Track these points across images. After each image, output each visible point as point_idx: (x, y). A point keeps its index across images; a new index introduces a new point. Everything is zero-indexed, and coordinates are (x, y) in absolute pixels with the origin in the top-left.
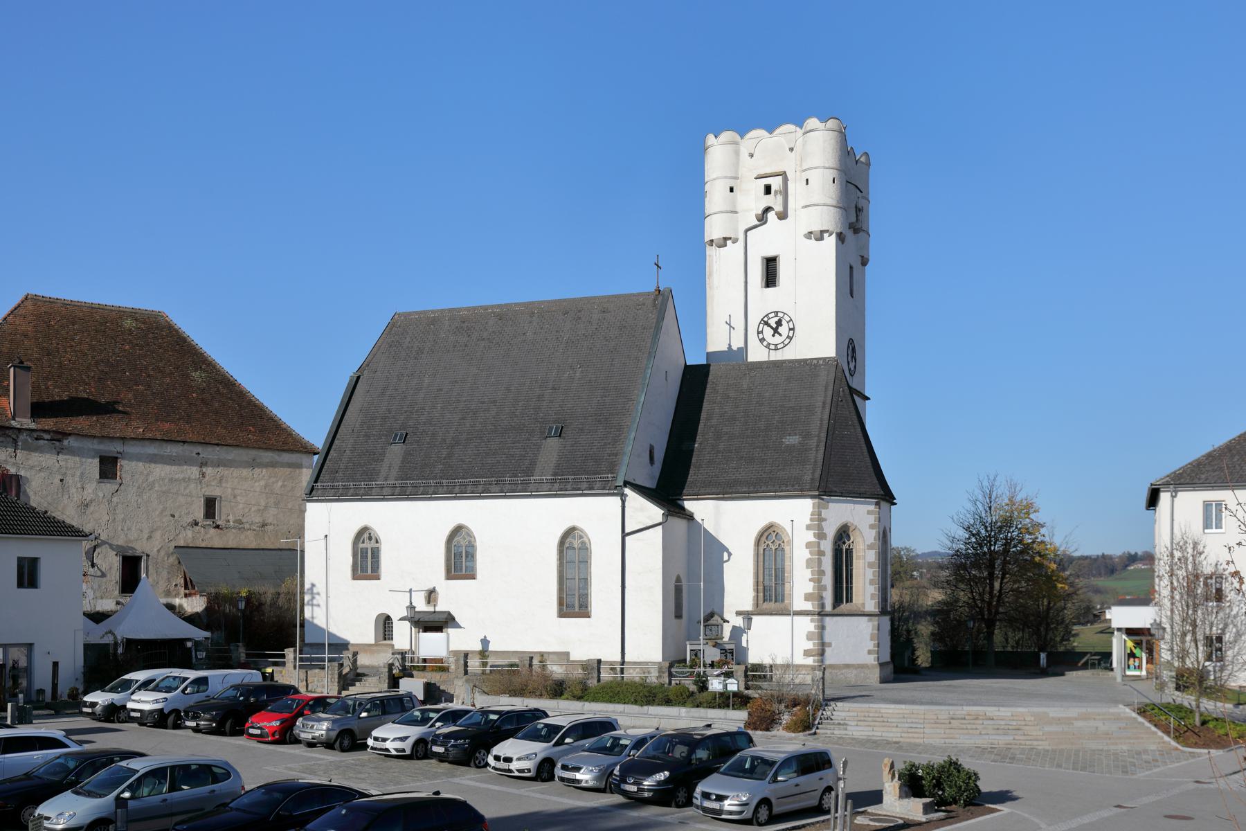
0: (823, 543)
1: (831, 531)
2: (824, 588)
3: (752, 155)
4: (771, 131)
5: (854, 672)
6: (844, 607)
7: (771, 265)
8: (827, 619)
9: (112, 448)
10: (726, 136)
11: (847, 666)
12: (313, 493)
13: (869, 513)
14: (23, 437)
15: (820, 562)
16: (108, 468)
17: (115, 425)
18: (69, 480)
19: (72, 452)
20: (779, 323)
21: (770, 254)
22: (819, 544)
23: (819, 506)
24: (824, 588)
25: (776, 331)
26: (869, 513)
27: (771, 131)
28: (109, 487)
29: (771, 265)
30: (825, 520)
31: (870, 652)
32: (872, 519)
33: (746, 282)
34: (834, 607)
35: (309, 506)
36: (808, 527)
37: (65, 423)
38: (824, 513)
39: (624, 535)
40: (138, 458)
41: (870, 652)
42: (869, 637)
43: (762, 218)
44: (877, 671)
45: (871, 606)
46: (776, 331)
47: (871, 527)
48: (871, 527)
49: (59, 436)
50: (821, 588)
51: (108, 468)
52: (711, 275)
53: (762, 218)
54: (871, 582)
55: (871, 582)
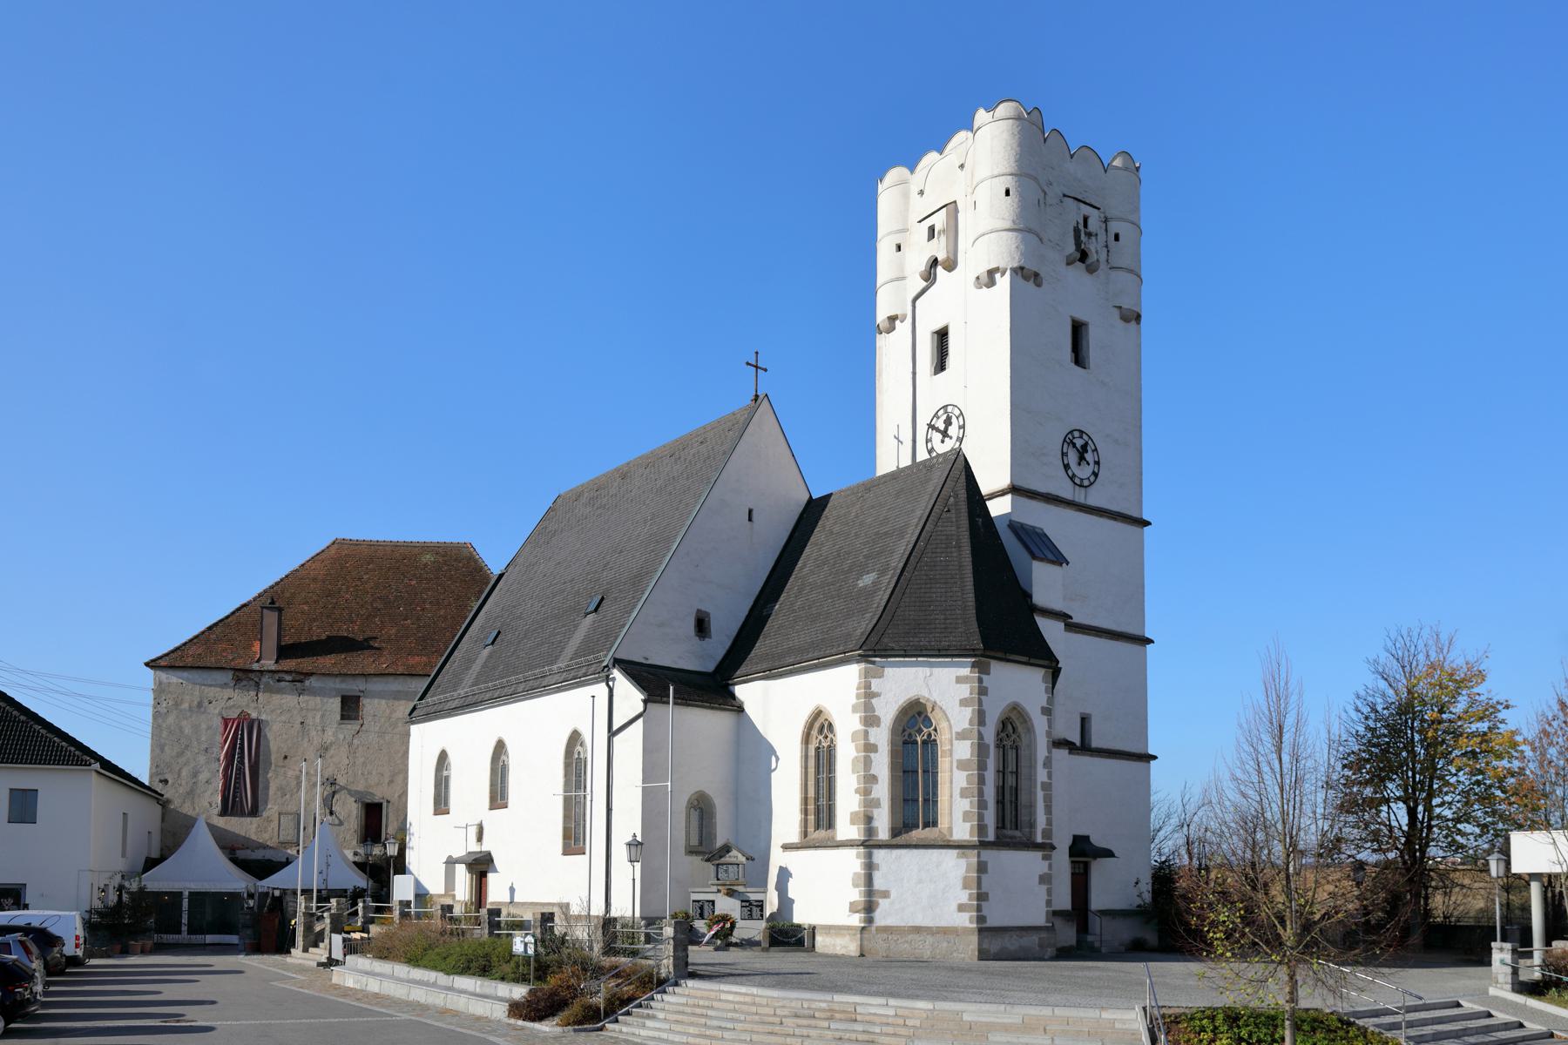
0: (873, 731)
1: (888, 711)
2: (876, 803)
3: (921, 193)
4: (941, 151)
5: (930, 939)
6: (918, 834)
7: (942, 336)
8: (880, 855)
9: (353, 686)
10: (895, 174)
11: (917, 930)
12: (414, 716)
13: (959, 680)
14: (265, 679)
15: (868, 763)
16: (350, 707)
17: (363, 661)
18: (309, 721)
19: (313, 692)
20: (948, 422)
21: (938, 326)
22: (866, 733)
23: (867, 675)
24: (876, 803)
25: (945, 434)
26: (959, 680)
27: (941, 151)
28: (352, 727)
31: (961, 908)
32: (965, 691)
33: (914, 373)
35: (414, 729)
36: (855, 709)
37: (306, 664)
38: (876, 685)
39: (612, 733)
40: (381, 695)
41: (961, 908)
42: (959, 884)
43: (929, 276)
44: (975, 938)
45: (963, 831)
46: (945, 434)
47: (964, 703)
48: (964, 703)
49: (300, 677)
50: (870, 803)
51: (350, 707)
53: (929, 276)
54: (964, 793)
55: (964, 793)
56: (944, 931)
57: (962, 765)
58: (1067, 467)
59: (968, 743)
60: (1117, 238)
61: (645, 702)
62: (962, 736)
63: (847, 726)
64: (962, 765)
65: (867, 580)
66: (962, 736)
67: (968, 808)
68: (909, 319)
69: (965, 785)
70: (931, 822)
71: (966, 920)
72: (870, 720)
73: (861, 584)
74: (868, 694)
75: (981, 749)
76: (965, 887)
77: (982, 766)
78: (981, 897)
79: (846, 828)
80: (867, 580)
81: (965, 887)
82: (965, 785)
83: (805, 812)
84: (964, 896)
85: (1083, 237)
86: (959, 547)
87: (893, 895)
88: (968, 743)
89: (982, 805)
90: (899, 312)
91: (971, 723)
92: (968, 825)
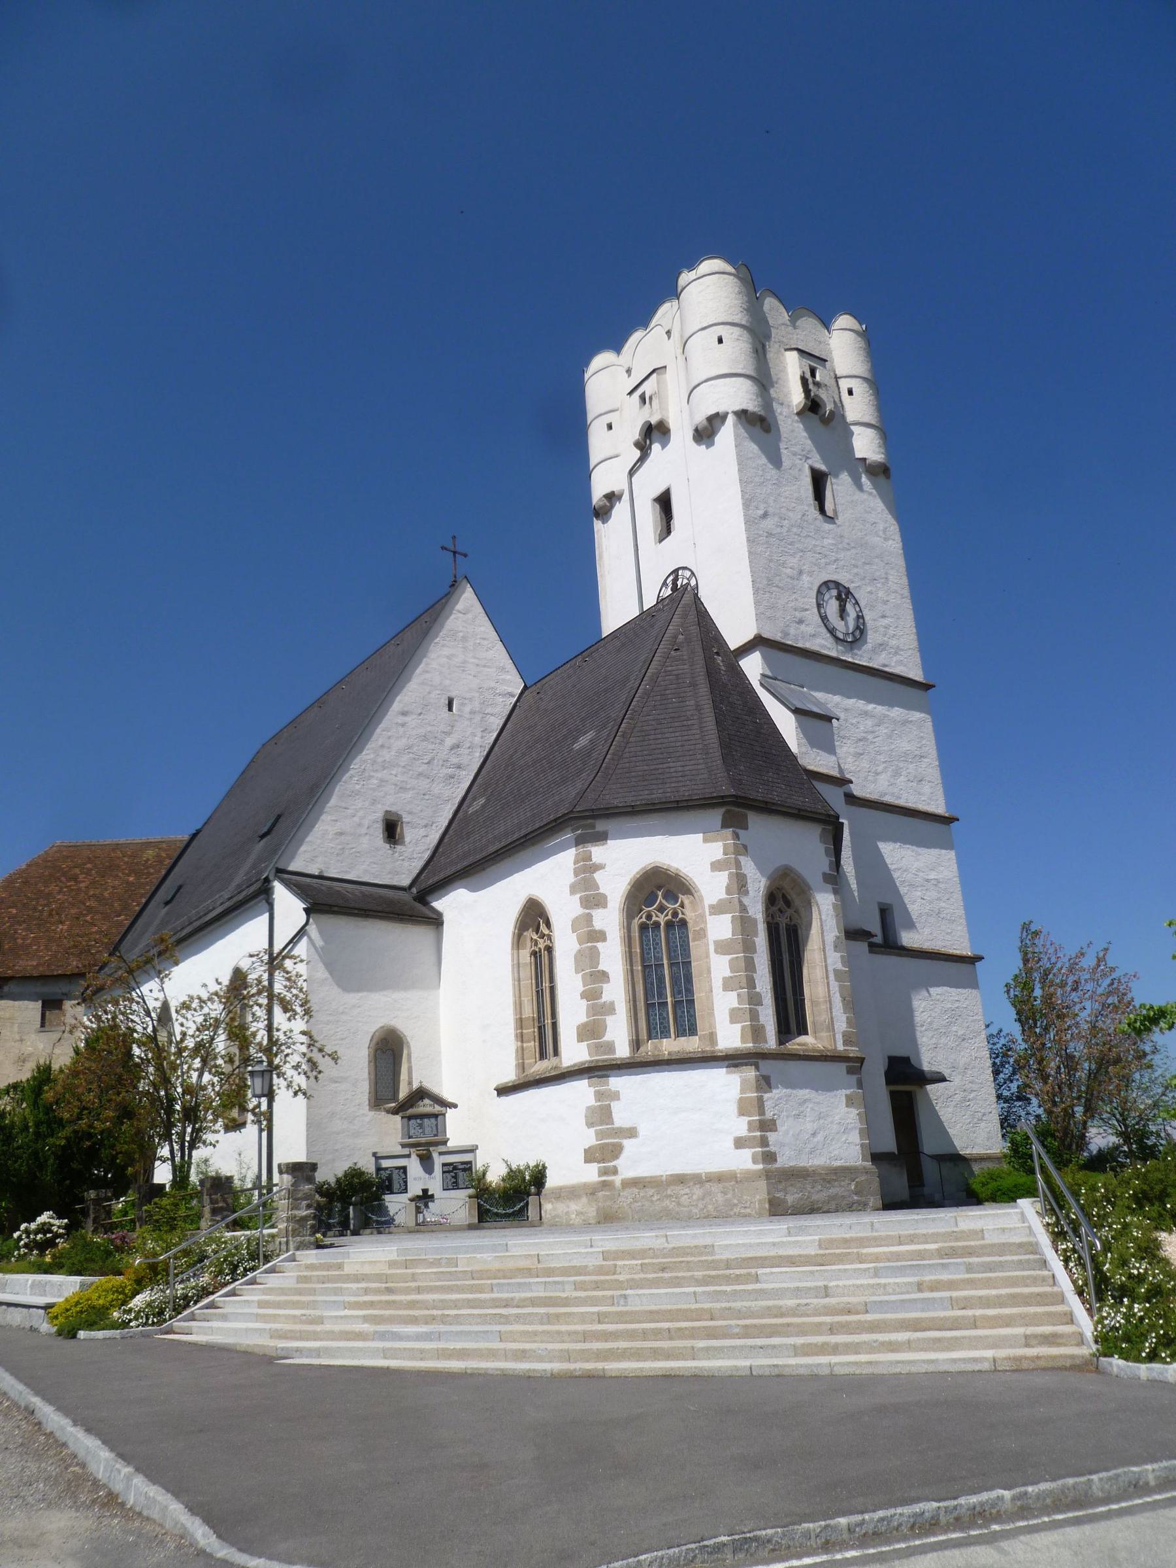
2: (610, 1009)
5: (698, 1192)
7: (664, 502)
8: (616, 1082)
11: (680, 1180)
22: (589, 919)
24: (610, 1009)
29: (664, 502)
30: (599, 867)
31: (739, 1143)
34: (636, 1044)
36: (573, 889)
41: (739, 1143)
42: (733, 1108)
44: (762, 1184)
47: (716, 866)
48: (716, 866)
50: (600, 1011)
52: (601, 557)
55: (727, 985)
56: (719, 1178)
57: (723, 947)
58: (824, 618)
59: (728, 917)
60: (850, 392)
61: (308, 911)
62: (718, 909)
63: (563, 910)
64: (723, 947)
65: (583, 741)
66: (718, 909)
67: (736, 1005)
68: (626, 497)
69: (728, 973)
70: (688, 1027)
71: (745, 1161)
72: (594, 900)
73: (576, 746)
74: (586, 870)
75: (744, 924)
76: (742, 1113)
77: (748, 947)
78: (767, 1125)
79: (573, 1052)
80: (583, 741)
81: (742, 1113)
82: (728, 973)
83: (521, 1037)
84: (741, 1126)
85: (811, 386)
86: (694, 685)
87: (642, 1132)
88: (728, 917)
89: (754, 1000)
90: (616, 489)
91: (728, 892)
92: (738, 1027)
